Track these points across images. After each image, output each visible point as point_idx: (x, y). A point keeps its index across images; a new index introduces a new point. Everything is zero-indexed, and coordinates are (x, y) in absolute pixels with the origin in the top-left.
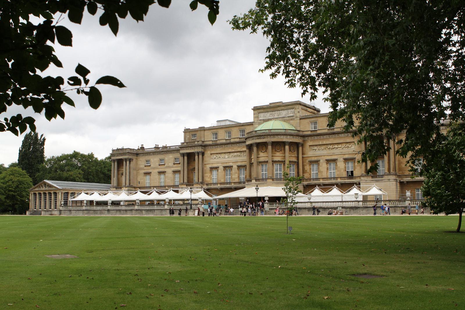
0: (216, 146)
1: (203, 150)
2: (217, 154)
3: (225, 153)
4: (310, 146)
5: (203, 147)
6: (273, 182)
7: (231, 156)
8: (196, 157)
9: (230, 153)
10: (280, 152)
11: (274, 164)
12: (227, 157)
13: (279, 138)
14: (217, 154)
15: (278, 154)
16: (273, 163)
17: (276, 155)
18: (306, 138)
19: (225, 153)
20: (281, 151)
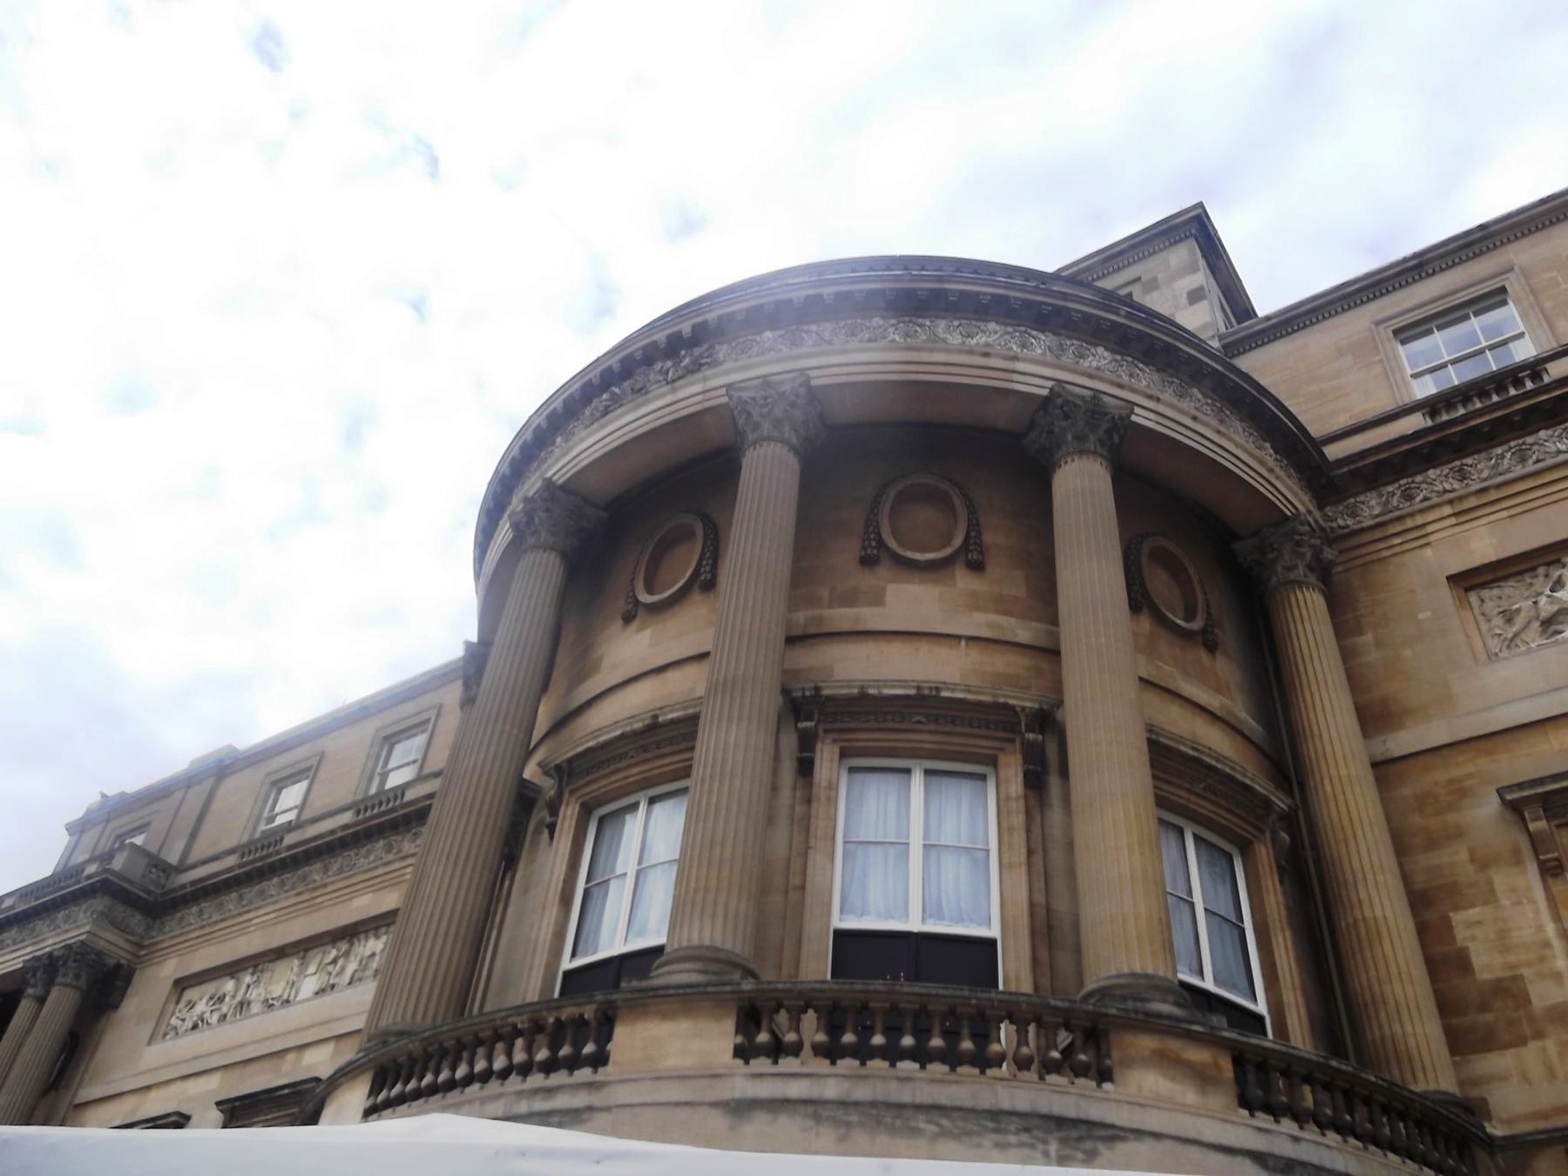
0: (250, 892)
1: (114, 944)
2: (232, 969)
3: (302, 948)
4: (1468, 581)
5: (136, 920)
6: (745, 1083)
7: (352, 966)
8: (25, 1007)
9: (350, 933)
10: (964, 580)
11: (826, 757)
12: (309, 985)
13: (935, 338)
14: (232, 969)
15: (909, 601)
16: (807, 743)
17: (872, 618)
18: (1371, 506)
19: (302, 948)
20: (977, 567)
